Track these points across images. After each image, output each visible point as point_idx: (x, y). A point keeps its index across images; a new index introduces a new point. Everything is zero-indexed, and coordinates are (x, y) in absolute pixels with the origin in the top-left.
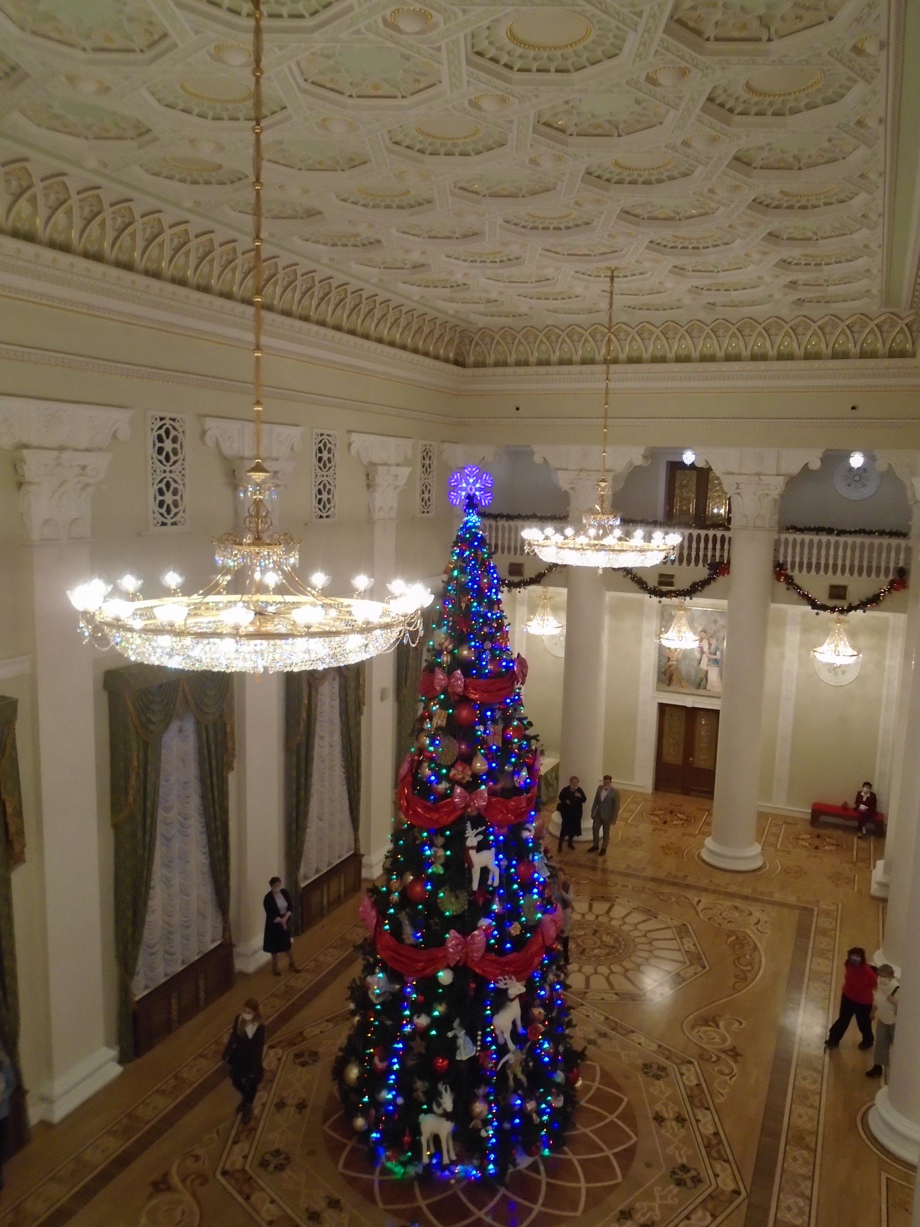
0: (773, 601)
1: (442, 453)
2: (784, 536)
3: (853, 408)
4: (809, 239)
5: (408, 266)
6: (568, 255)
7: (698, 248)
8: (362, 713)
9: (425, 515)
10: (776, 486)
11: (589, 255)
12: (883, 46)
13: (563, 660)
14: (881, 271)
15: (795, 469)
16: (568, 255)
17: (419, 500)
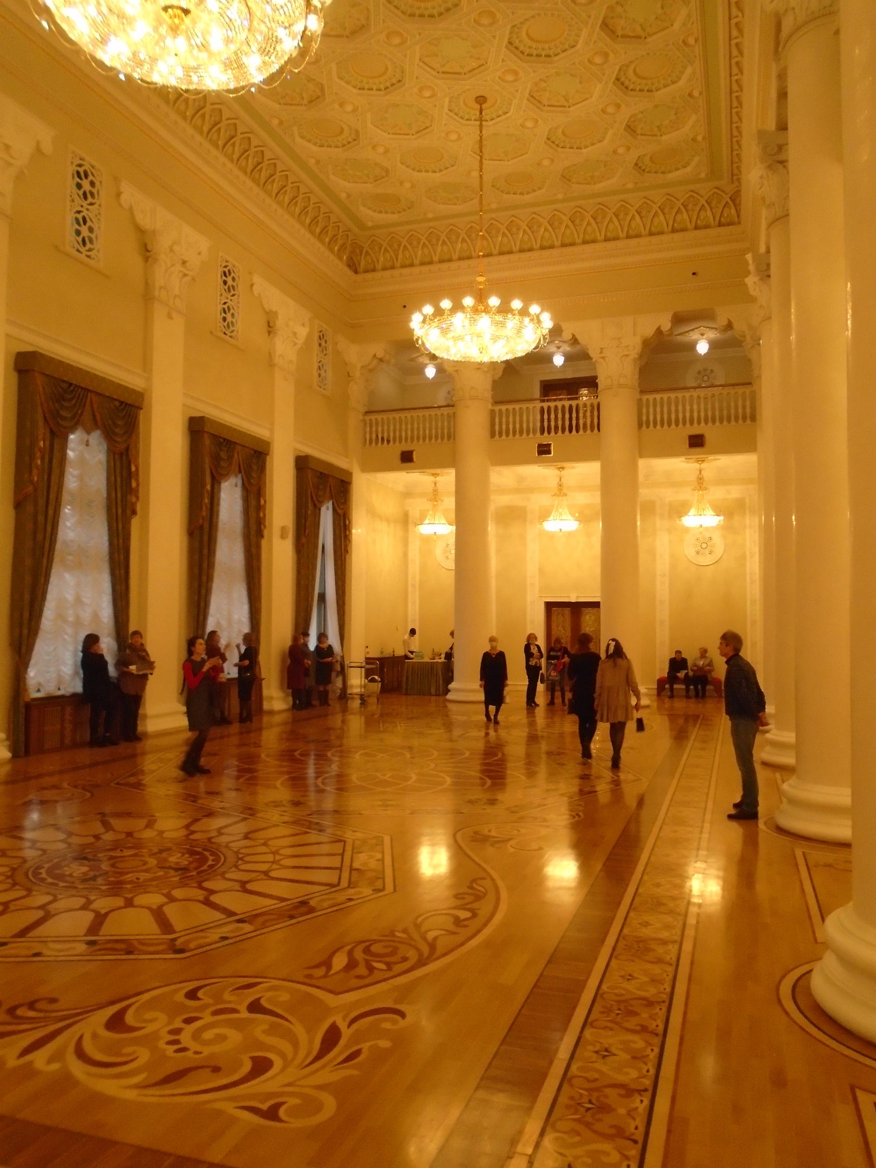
0: (641, 457)
1: (336, 343)
2: (645, 397)
3: (694, 274)
4: (640, 37)
5: (305, 102)
6: (444, 73)
7: (549, 56)
8: (262, 536)
9: (321, 390)
10: (633, 344)
11: (460, 74)
12: (696, 41)
13: (453, 573)
14: (704, 138)
15: (650, 332)
16: (444, 73)
17: (316, 375)
